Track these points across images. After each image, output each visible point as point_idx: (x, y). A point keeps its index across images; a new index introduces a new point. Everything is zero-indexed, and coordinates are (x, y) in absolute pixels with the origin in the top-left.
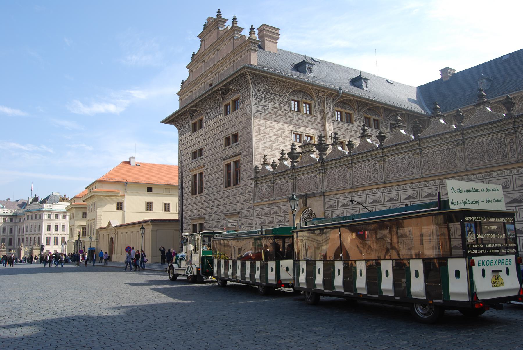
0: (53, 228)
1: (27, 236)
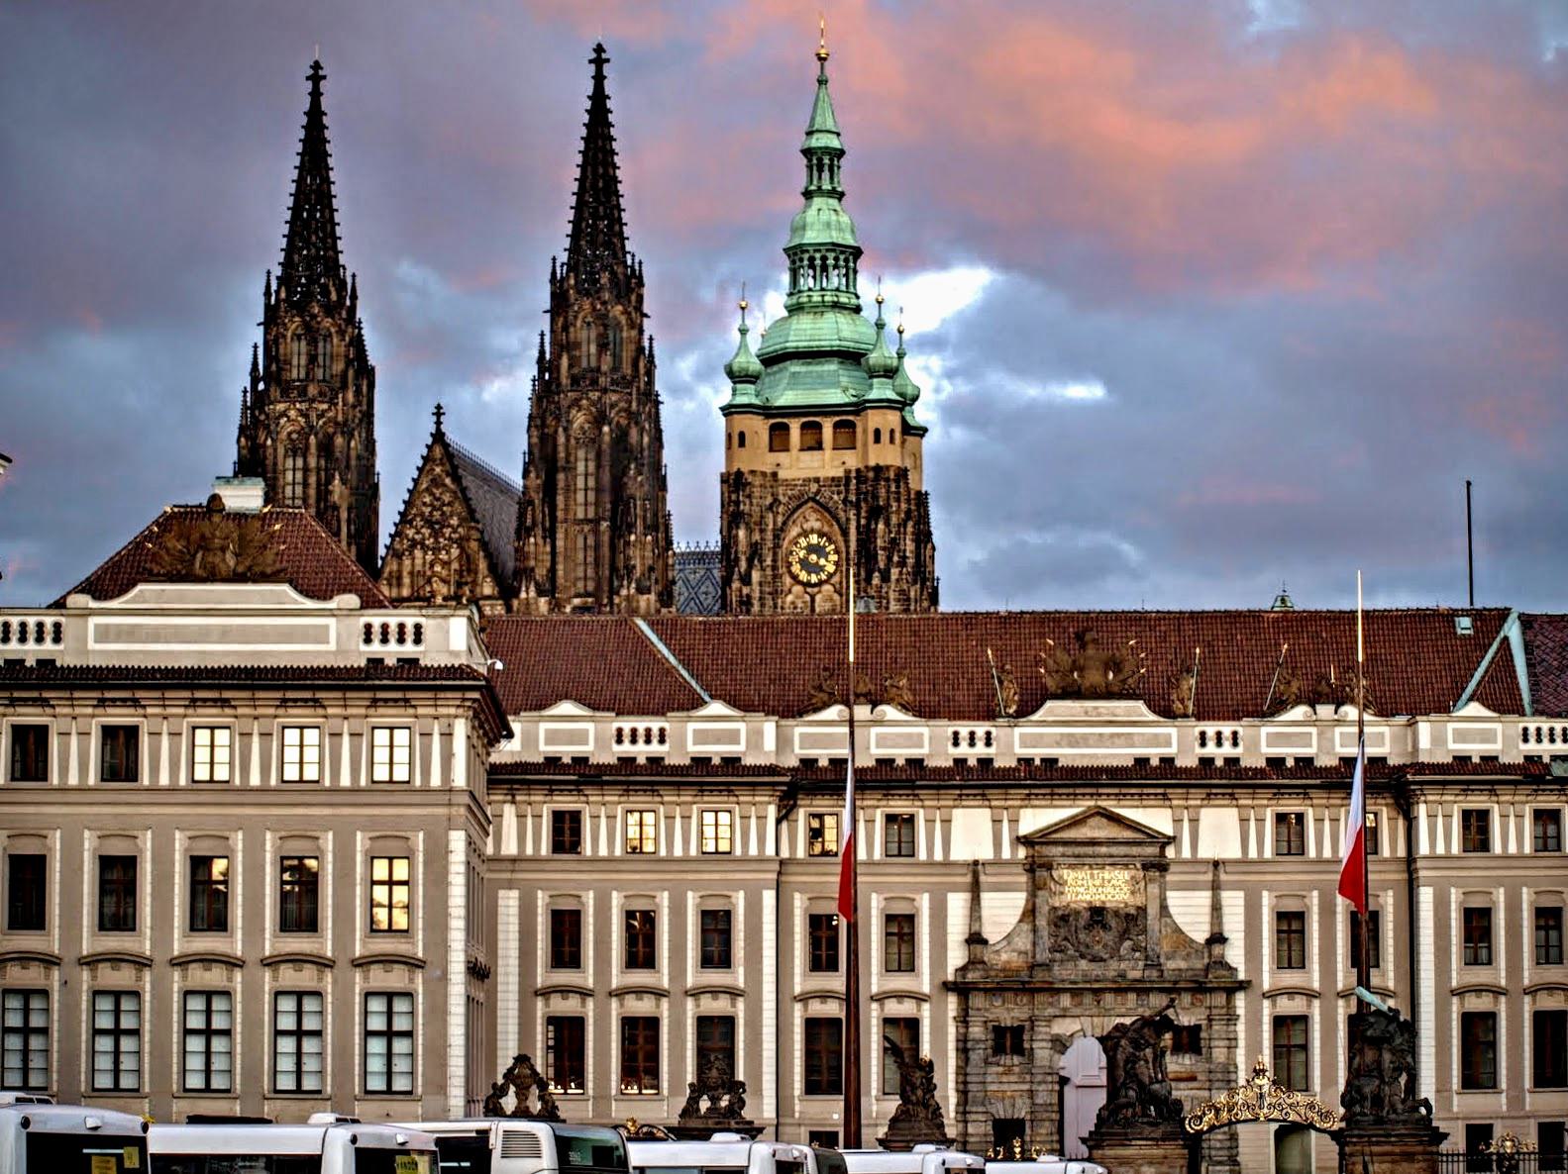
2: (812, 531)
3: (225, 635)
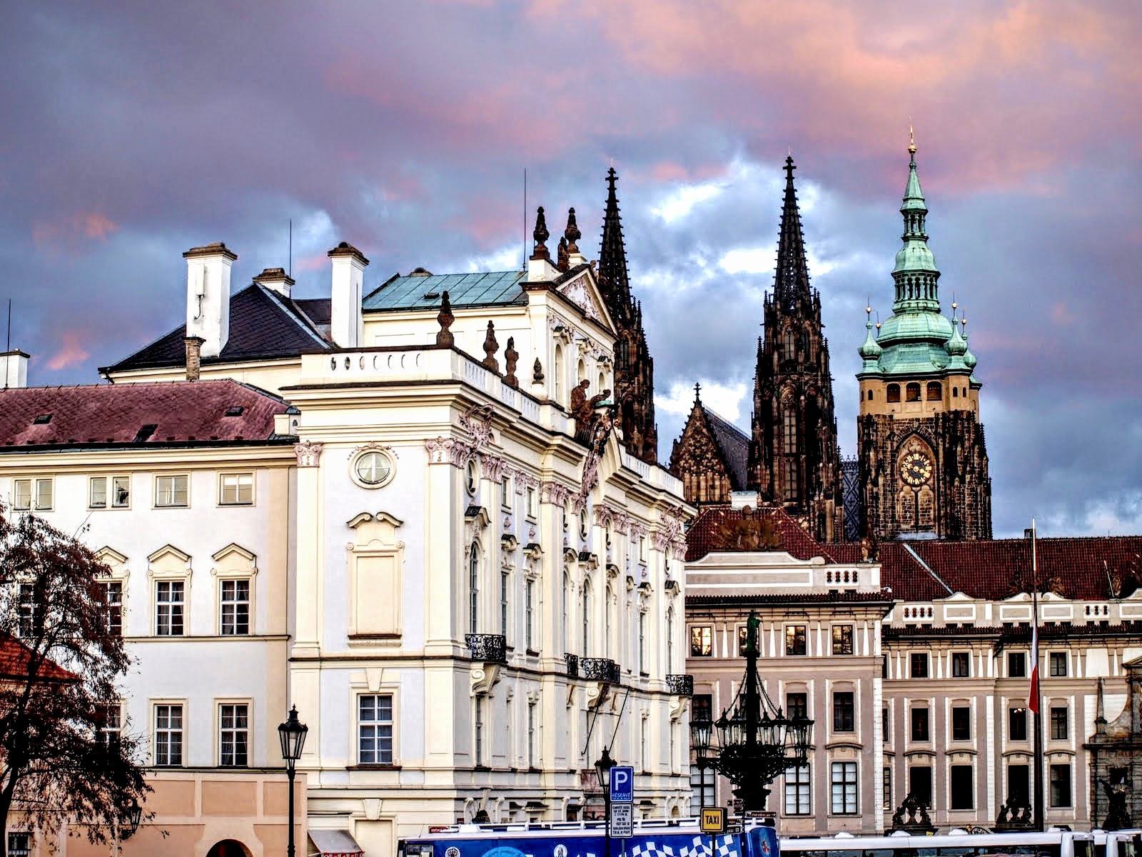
2: (915, 452)
3: (755, 579)
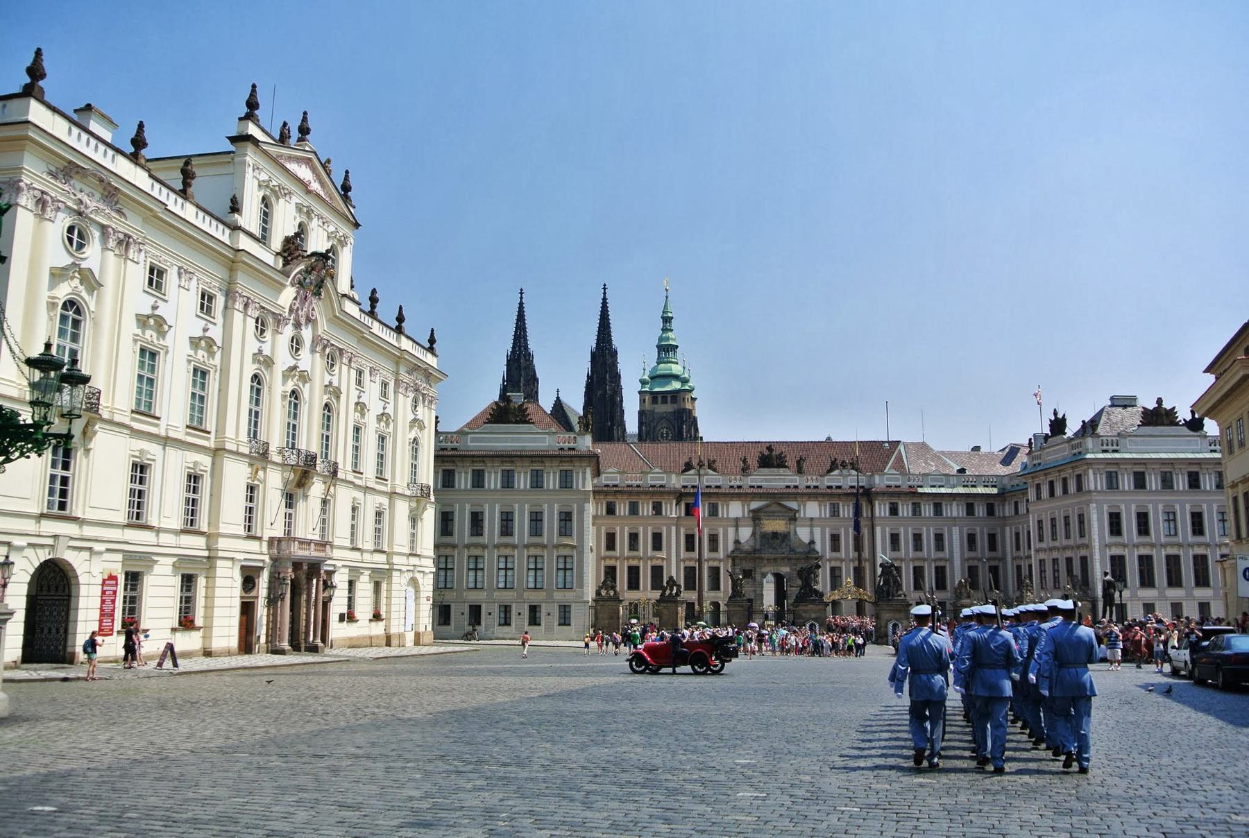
0: (1129, 524)
1: (1042, 556)
3: (513, 440)
